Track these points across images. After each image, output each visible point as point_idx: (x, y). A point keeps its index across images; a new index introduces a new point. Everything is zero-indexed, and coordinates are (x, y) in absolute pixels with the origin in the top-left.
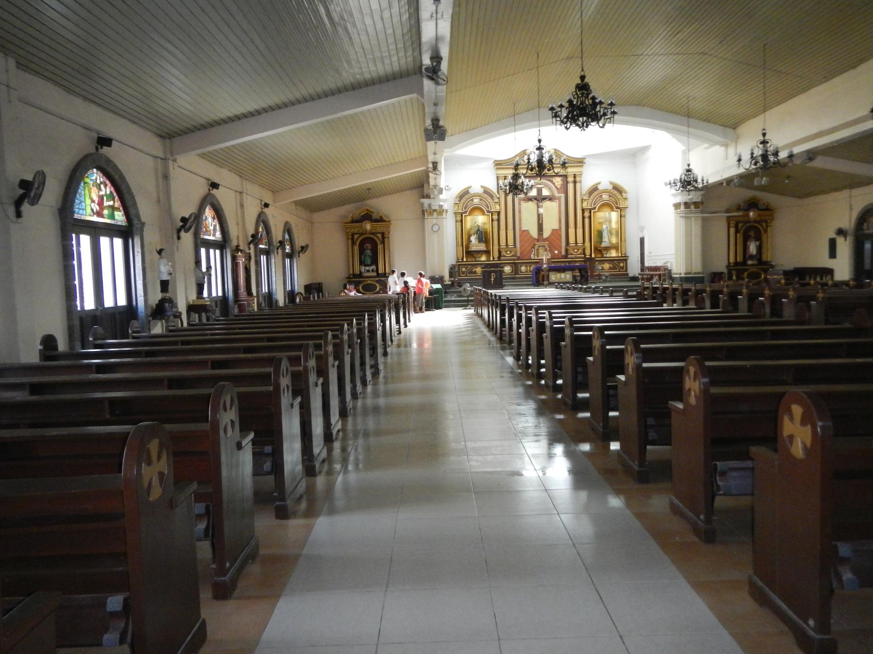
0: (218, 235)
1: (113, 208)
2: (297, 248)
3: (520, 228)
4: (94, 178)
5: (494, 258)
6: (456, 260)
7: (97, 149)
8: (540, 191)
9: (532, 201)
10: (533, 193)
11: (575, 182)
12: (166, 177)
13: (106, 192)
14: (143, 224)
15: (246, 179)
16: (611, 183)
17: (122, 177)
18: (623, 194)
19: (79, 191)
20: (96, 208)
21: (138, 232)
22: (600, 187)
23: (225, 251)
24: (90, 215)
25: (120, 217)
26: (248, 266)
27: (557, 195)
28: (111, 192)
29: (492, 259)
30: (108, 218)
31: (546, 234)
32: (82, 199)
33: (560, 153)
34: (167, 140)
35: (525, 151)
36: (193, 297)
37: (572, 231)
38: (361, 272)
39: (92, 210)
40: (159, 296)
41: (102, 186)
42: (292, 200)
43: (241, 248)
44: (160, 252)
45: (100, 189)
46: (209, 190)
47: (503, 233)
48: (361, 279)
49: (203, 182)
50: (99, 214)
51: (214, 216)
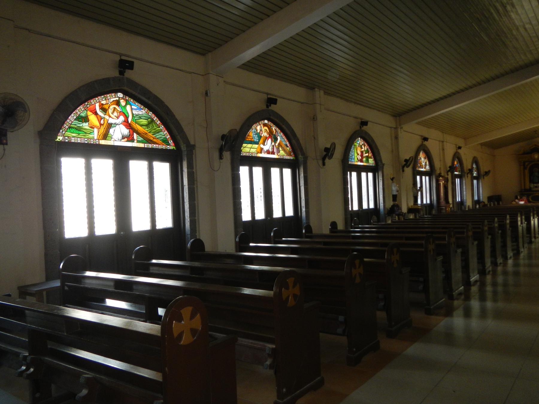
0: (428, 167)
1: (368, 157)
2: (482, 172)
4: (359, 142)
7: (361, 127)
12: (396, 138)
13: (365, 149)
14: (383, 165)
15: (446, 133)
17: (373, 140)
19: (352, 150)
20: (360, 157)
21: (381, 169)
23: (432, 177)
24: (356, 162)
25: (371, 161)
26: (446, 186)
28: (367, 149)
30: (365, 163)
32: (353, 154)
34: (398, 118)
36: (411, 204)
38: (530, 188)
39: (358, 159)
40: (392, 203)
41: (363, 146)
42: (478, 143)
43: (442, 175)
44: (392, 179)
45: (362, 148)
46: (422, 142)
48: (530, 193)
49: (419, 137)
50: (361, 161)
51: (425, 157)
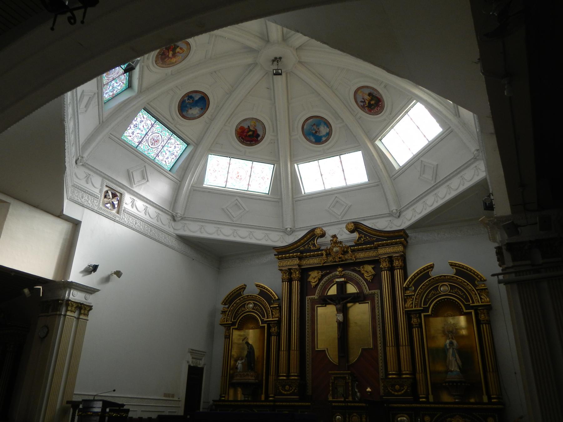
3: (313, 348)
5: (267, 396)
6: (217, 398)
8: (342, 287)
9: (329, 304)
10: (333, 291)
11: (391, 269)
16: (452, 265)
18: (476, 282)
22: (434, 274)
27: (367, 291)
29: (263, 397)
31: (353, 358)
33: (362, 228)
35: (313, 230)
37: (390, 350)
47: (283, 354)
